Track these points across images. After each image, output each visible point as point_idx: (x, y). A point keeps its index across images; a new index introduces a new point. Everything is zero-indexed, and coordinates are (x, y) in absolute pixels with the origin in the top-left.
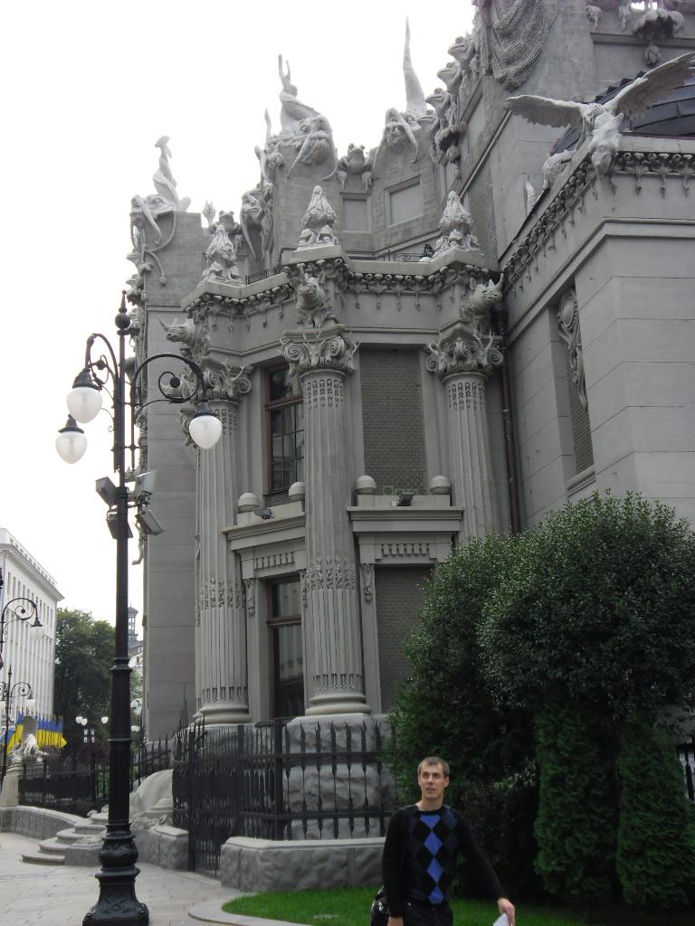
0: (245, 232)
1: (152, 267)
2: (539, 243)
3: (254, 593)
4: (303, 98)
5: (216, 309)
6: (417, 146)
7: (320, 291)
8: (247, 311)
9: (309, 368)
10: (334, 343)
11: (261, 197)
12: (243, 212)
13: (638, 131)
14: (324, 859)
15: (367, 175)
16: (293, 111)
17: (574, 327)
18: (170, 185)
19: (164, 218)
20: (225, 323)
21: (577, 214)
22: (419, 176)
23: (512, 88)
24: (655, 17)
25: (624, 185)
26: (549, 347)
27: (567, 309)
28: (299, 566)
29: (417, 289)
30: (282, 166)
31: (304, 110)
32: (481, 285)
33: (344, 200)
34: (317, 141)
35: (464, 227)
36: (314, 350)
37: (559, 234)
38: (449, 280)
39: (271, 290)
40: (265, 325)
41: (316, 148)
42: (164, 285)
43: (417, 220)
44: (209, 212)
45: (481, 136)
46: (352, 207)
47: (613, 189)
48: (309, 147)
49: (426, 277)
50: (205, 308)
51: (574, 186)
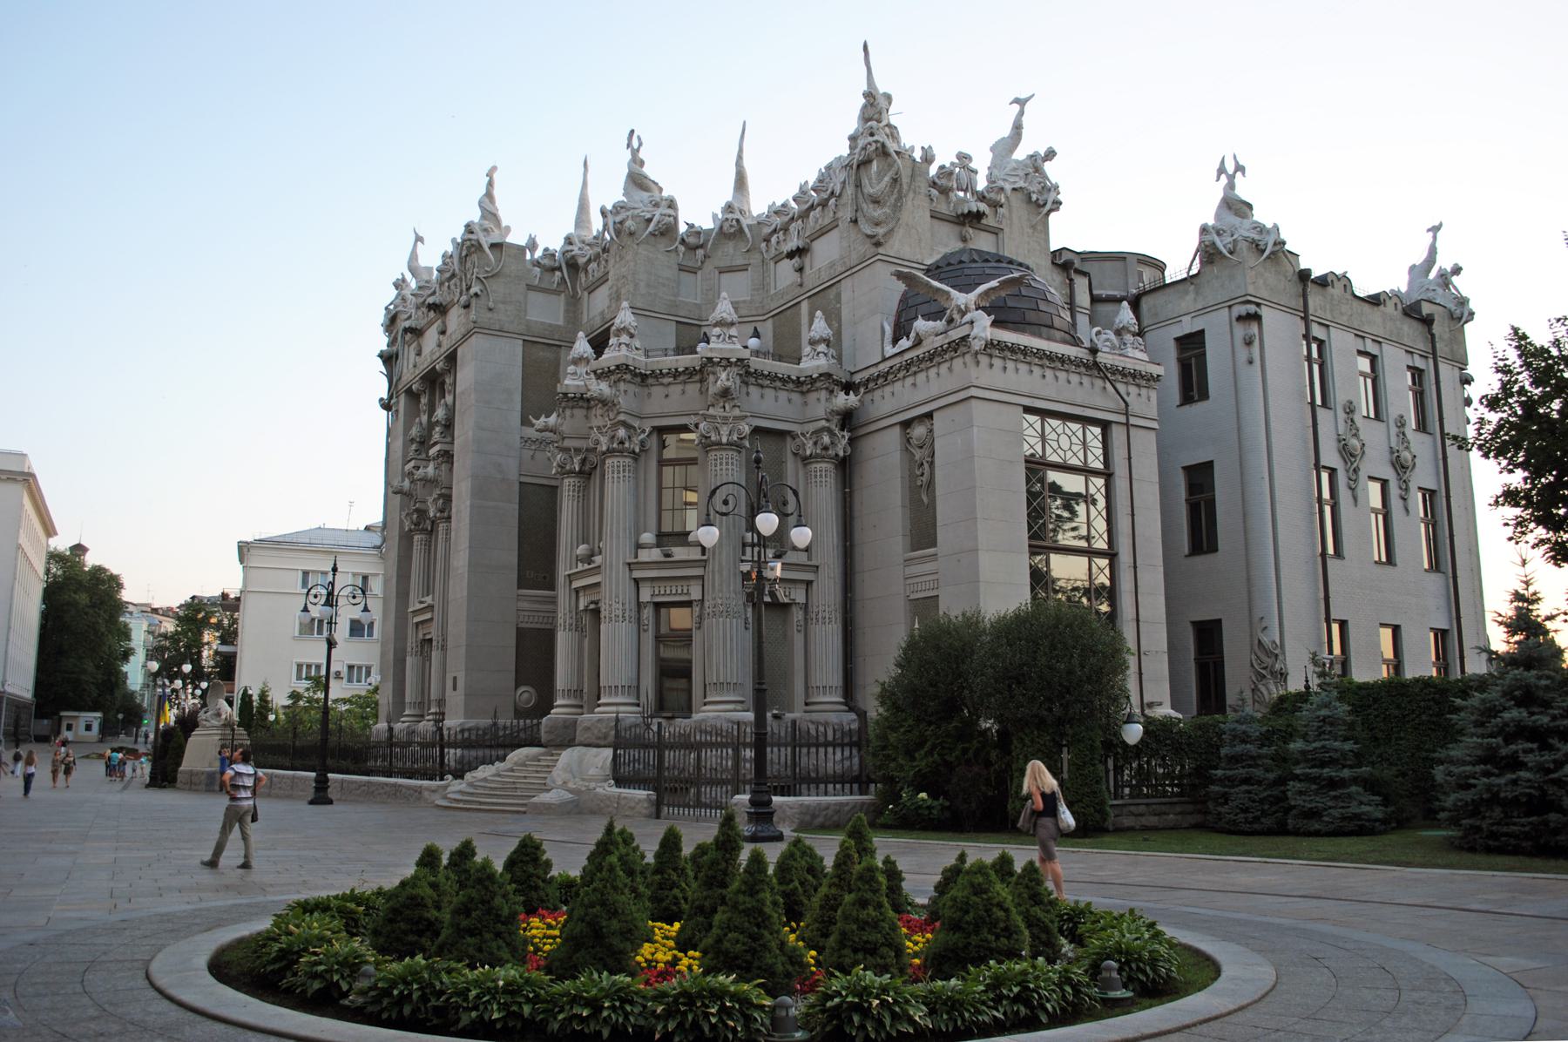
2: (900, 375)
3: (648, 613)
4: (649, 170)
5: (628, 377)
8: (650, 381)
9: (719, 443)
11: (599, 250)
13: (995, 324)
14: (827, 808)
15: (700, 252)
16: (637, 180)
17: (928, 444)
19: (493, 246)
20: (632, 388)
21: (944, 368)
23: (878, 244)
25: (984, 360)
26: (897, 455)
27: (919, 431)
28: (695, 594)
29: (791, 386)
30: (631, 234)
35: (827, 342)
36: (725, 431)
37: (921, 377)
38: (818, 384)
44: (532, 245)
45: (832, 265)
46: (684, 275)
47: (978, 363)
51: (945, 351)
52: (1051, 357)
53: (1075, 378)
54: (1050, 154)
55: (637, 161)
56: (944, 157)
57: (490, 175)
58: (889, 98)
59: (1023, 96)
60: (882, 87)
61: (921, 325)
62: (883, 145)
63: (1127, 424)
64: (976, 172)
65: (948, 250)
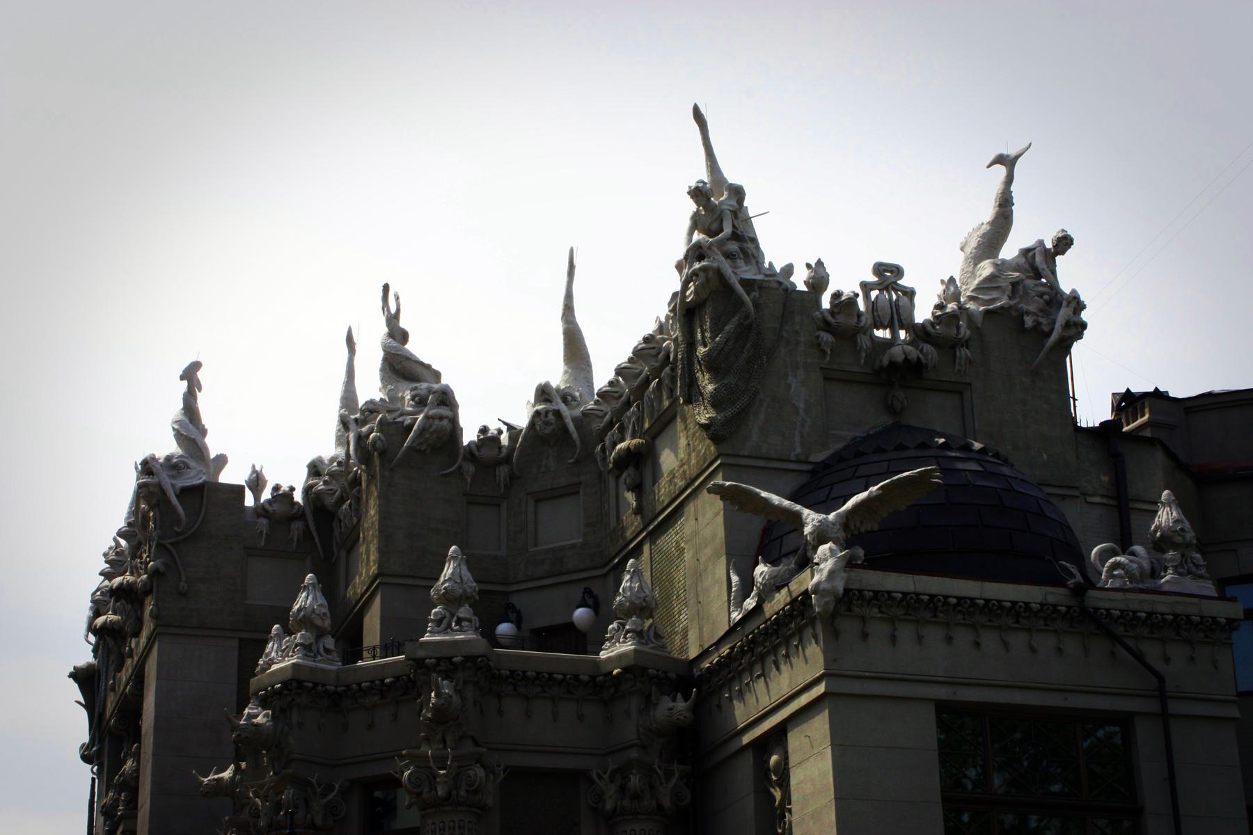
0: (310, 518)
1: (165, 564)
4: (417, 347)
6: (578, 442)
7: (456, 699)
10: (471, 773)
12: (307, 490)
15: (503, 471)
18: (198, 438)
19: (187, 493)
22: (580, 483)
24: (900, 358)
25: (849, 627)
31: (419, 369)
32: (666, 698)
33: (469, 503)
34: (437, 422)
39: (382, 681)
40: (370, 726)
41: (435, 431)
42: (182, 595)
43: (573, 546)
44: (257, 482)
48: (423, 430)
49: (593, 678)
50: (289, 699)
52: (992, 609)
53: (1046, 643)
54: (1064, 243)
55: (397, 334)
56: (848, 278)
57: (191, 374)
58: (738, 193)
59: (1012, 152)
60: (732, 176)
61: (762, 570)
62: (719, 273)
63: (1165, 717)
64: (910, 294)
65: (859, 433)
